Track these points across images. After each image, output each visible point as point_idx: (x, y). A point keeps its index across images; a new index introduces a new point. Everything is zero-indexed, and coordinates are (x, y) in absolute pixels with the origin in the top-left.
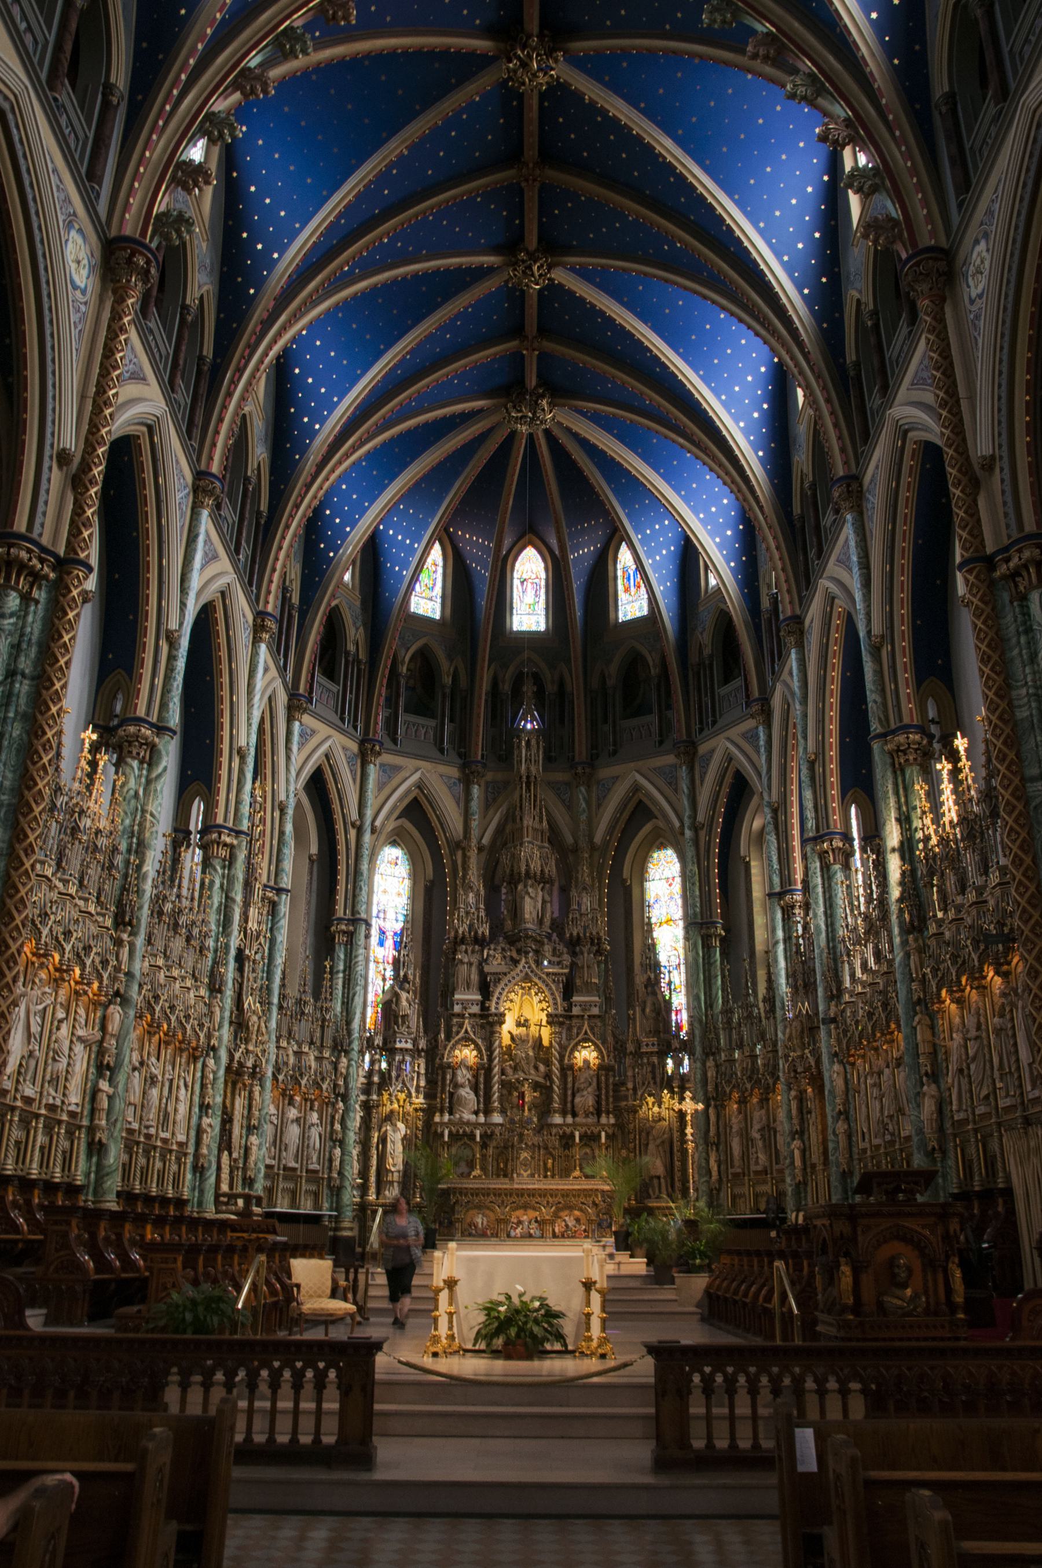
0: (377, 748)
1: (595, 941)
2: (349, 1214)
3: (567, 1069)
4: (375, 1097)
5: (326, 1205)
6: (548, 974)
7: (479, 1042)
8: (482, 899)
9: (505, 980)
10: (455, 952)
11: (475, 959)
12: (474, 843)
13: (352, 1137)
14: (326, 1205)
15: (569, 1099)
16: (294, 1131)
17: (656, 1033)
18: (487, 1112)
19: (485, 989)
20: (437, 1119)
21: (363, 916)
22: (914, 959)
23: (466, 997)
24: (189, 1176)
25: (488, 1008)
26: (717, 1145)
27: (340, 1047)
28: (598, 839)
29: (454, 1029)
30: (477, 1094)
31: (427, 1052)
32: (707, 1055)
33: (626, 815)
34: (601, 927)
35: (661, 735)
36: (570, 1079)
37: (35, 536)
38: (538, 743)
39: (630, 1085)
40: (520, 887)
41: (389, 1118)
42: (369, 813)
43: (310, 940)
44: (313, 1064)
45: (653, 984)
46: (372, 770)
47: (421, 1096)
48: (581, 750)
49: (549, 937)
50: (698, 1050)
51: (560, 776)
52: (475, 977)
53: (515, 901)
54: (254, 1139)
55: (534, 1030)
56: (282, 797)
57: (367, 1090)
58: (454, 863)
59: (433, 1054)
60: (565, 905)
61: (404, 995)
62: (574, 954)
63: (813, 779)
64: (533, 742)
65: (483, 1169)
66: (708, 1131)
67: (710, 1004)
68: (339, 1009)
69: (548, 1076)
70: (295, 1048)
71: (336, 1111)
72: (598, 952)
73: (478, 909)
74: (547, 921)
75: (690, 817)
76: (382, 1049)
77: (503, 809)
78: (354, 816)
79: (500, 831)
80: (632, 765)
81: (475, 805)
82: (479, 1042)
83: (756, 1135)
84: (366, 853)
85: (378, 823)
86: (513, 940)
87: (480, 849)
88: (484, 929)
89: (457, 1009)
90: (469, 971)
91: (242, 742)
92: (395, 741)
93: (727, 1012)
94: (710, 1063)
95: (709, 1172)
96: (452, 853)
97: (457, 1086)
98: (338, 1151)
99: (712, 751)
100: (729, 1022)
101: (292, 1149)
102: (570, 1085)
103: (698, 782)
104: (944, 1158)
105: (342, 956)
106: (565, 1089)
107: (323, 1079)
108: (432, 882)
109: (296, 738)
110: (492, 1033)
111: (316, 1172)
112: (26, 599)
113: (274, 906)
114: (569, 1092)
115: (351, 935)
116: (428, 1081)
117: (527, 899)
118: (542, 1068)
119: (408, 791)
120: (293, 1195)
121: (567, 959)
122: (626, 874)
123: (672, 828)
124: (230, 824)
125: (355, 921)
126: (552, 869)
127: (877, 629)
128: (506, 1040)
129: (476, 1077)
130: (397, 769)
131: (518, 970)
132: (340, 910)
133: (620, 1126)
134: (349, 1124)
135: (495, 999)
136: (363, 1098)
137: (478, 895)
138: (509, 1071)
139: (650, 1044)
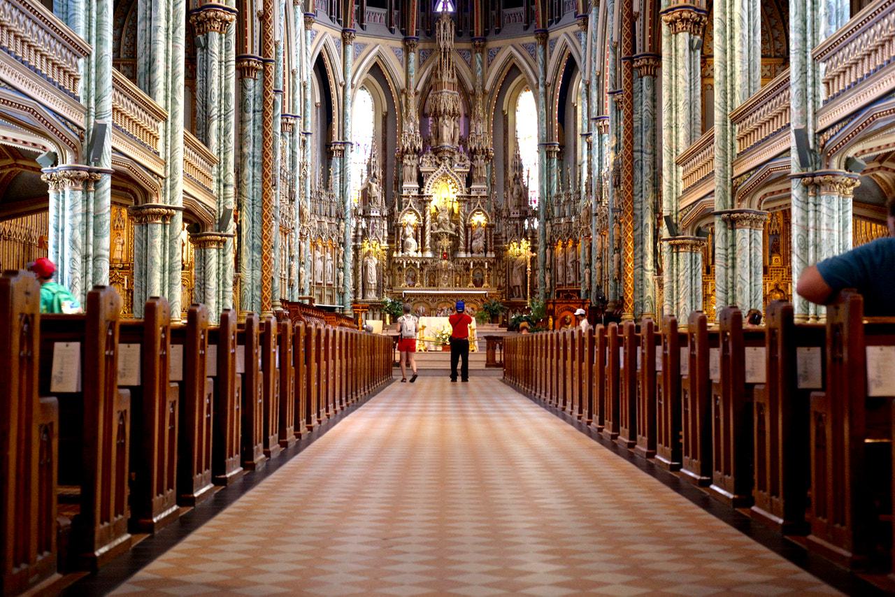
0: (353, 35)
1: (485, 152)
2: (348, 307)
3: (468, 227)
4: (360, 244)
5: (337, 302)
6: (457, 172)
7: (418, 211)
8: (417, 127)
9: (432, 176)
10: (402, 157)
11: (414, 163)
12: (412, 91)
13: (349, 266)
14: (337, 302)
15: (469, 243)
16: (319, 264)
17: (519, 206)
18: (423, 251)
19: (421, 181)
20: (395, 255)
21: (349, 140)
22: (615, 198)
23: (410, 186)
24: (287, 290)
25: (423, 193)
26: (550, 270)
27: (340, 217)
28: (488, 88)
29: (403, 205)
30: (417, 241)
31: (387, 217)
32: (547, 220)
33: (505, 73)
34: (488, 144)
35: (527, 22)
36: (470, 232)
37: (254, 55)
38: (451, 26)
39: (504, 235)
40: (441, 119)
41: (368, 254)
42: (349, 76)
43: (318, 154)
44: (327, 227)
45: (518, 178)
46: (350, 49)
47: (385, 242)
48: (478, 30)
49: (458, 149)
50: (542, 217)
51: (464, 46)
52: (415, 174)
53: (437, 128)
54: (302, 269)
55: (449, 205)
56: (305, 79)
57: (355, 240)
58: (400, 103)
59: (391, 217)
60: (468, 128)
61: (374, 185)
62: (472, 160)
63: (598, 85)
64: (448, 26)
65: (422, 282)
66: (545, 262)
67: (549, 192)
68: (338, 195)
69: (457, 230)
70: (318, 219)
71: (340, 252)
72: (487, 158)
73: (415, 132)
74: (457, 139)
75: (542, 79)
76: (363, 217)
77: (430, 67)
78: (341, 79)
79: (428, 81)
80: (509, 41)
81: (412, 66)
82: (418, 211)
83: (569, 265)
84: (349, 101)
85: (355, 82)
86: (436, 151)
87: (416, 94)
88: (420, 145)
89: (405, 193)
90: (411, 170)
91: (294, 67)
92: (362, 27)
93: (558, 196)
94: (548, 225)
95: (545, 284)
96: (399, 97)
97: (406, 237)
98: (342, 274)
99: (557, 38)
100: (559, 202)
101: (319, 274)
102: (470, 236)
103: (548, 57)
104: (620, 282)
105: (338, 164)
106: (467, 238)
107: (333, 235)
108: (387, 113)
109: (309, 41)
110: (425, 206)
111: (331, 285)
112: (255, 79)
113: (304, 142)
114: (469, 240)
115: (343, 152)
116: (389, 234)
117: (445, 127)
118: (454, 226)
119: (372, 59)
120: (321, 297)
121: (468, 163)
122: (505, 108)
123: (532, 83)
124: (291, 114)
125: (344, 144)
126: (460, 108)
127: (615, 39)
128: (434, 210)
129: (416, 231)
130: (365, 45)
131: (439, 170)
132: (336, 137)
133: (498, 258)
134: (347, 258)
135: (426, 187)
136: (354, 244)
137: (415, 123)
138: (435, 228)
139: (515, 214)
